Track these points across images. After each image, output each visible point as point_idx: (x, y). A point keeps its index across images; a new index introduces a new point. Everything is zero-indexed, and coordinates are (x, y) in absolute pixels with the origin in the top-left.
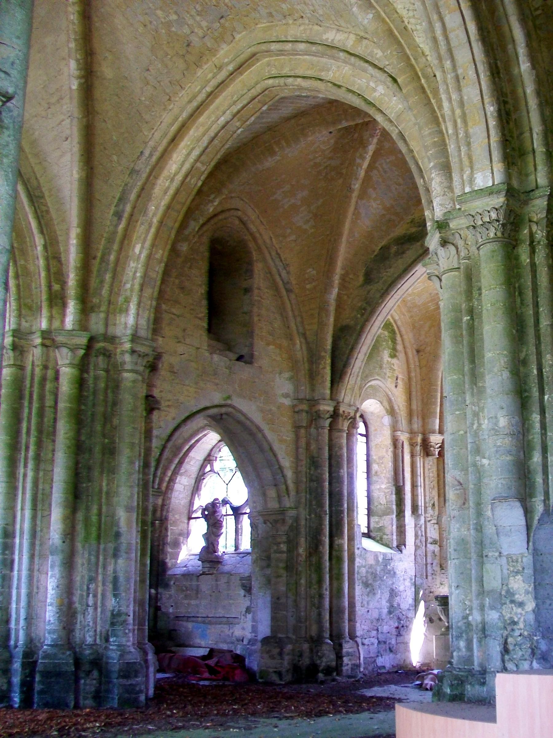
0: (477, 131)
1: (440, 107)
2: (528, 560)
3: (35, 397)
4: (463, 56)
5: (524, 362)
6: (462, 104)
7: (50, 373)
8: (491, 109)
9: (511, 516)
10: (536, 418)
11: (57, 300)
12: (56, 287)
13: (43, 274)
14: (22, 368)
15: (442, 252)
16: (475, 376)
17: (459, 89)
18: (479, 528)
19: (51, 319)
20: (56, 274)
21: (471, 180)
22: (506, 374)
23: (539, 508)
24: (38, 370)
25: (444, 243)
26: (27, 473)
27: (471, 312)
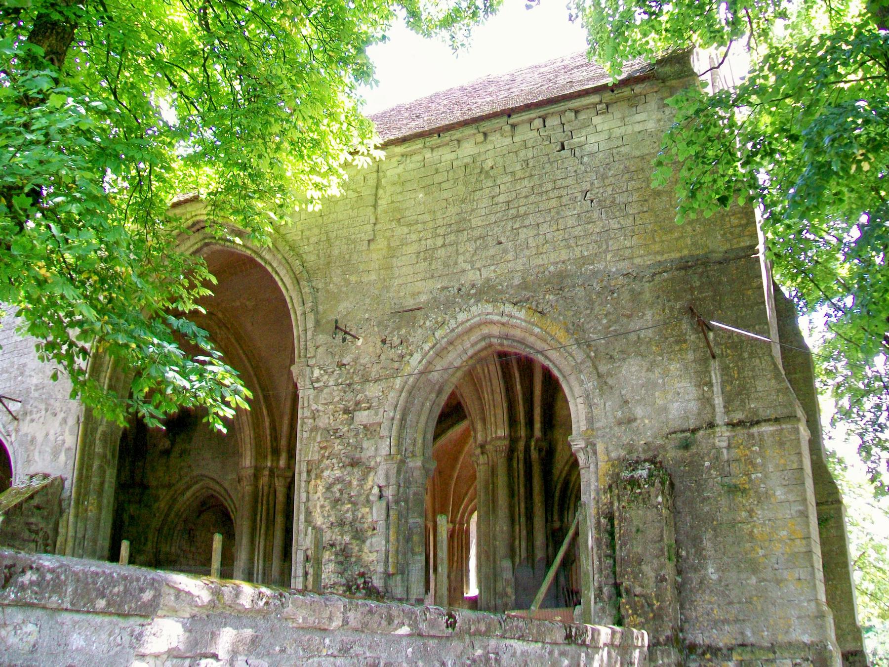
0: (499, 412)
1: (483, 392)
2: (513, 580)
3: (264, 502)
4: (495, 382)
5: (514, 507)
6: (493, 400)
7: (272, 490)
8: (505, 405)
9: (507, 564)
10: (517, 527)
11: (276, 452)
12: (275, 444)
13: (269, 438)
14: (257, 487)
15: (481, 457)
16: (494, 510)
17: (493, 394)
18: (494, 568)
19: (272, 461)
20: (275, 438)
21: (496, 432)
22: (507, 511)
23: (517, 560)
24: (266, 488)
25: (482, 453)
26: (261, 542)
27: (493, 483)
